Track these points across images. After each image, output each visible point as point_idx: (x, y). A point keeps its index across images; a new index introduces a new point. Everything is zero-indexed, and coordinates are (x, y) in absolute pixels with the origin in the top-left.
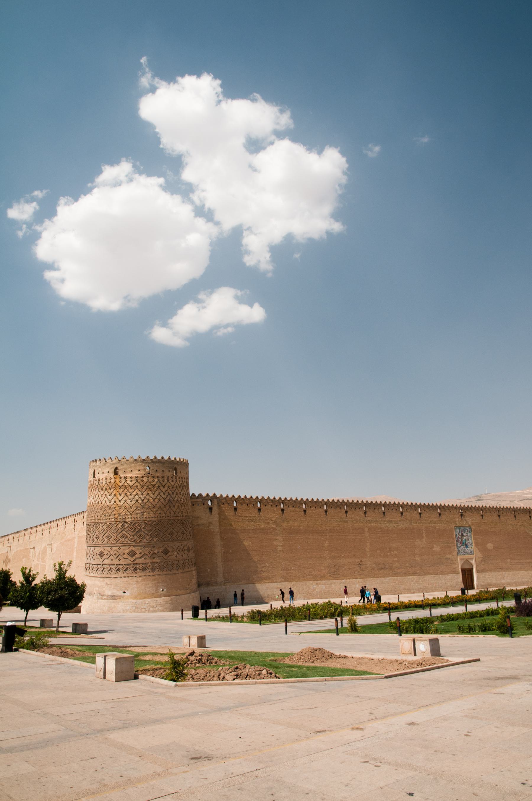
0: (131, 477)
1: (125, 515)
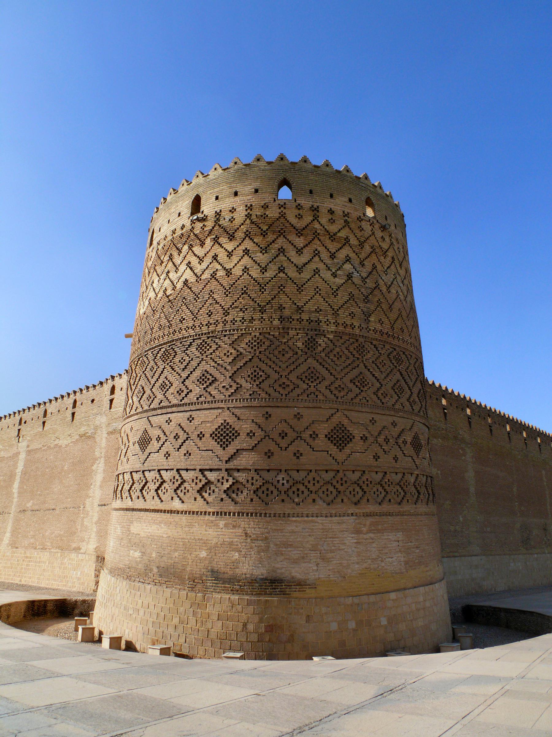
0: (331, 212)
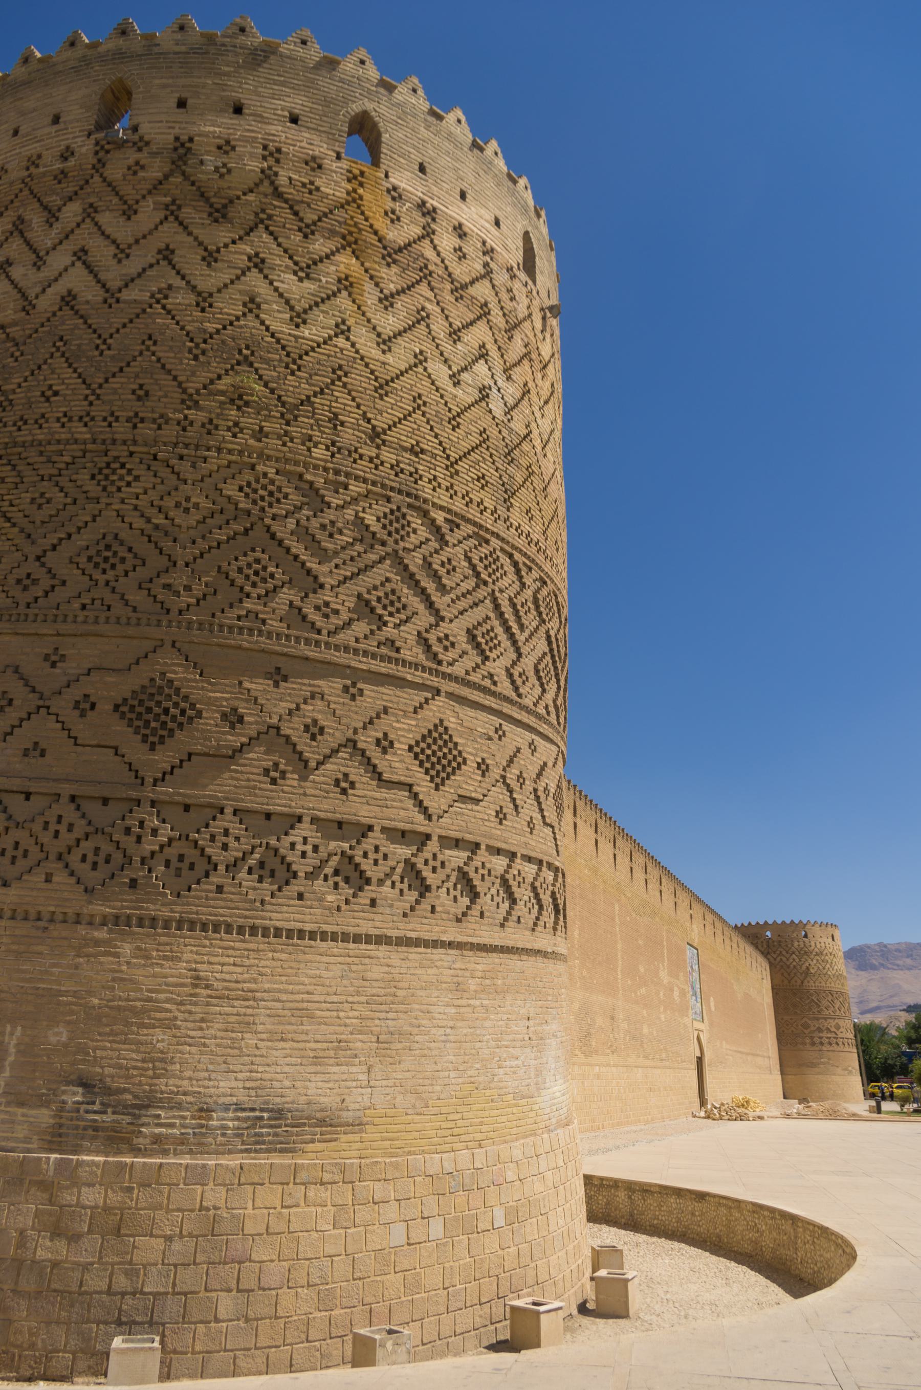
0: (460, 231)
1: (412, 450)
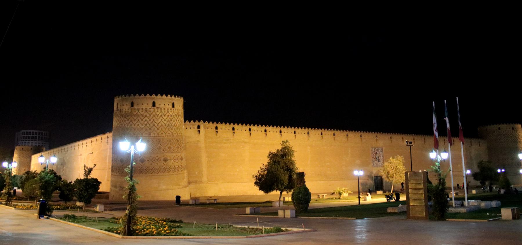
0: (142, 109)
